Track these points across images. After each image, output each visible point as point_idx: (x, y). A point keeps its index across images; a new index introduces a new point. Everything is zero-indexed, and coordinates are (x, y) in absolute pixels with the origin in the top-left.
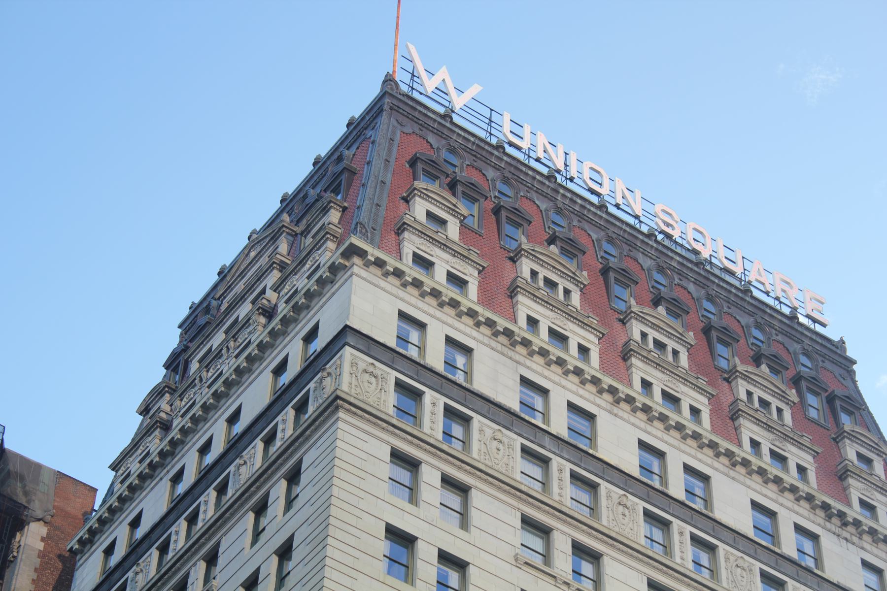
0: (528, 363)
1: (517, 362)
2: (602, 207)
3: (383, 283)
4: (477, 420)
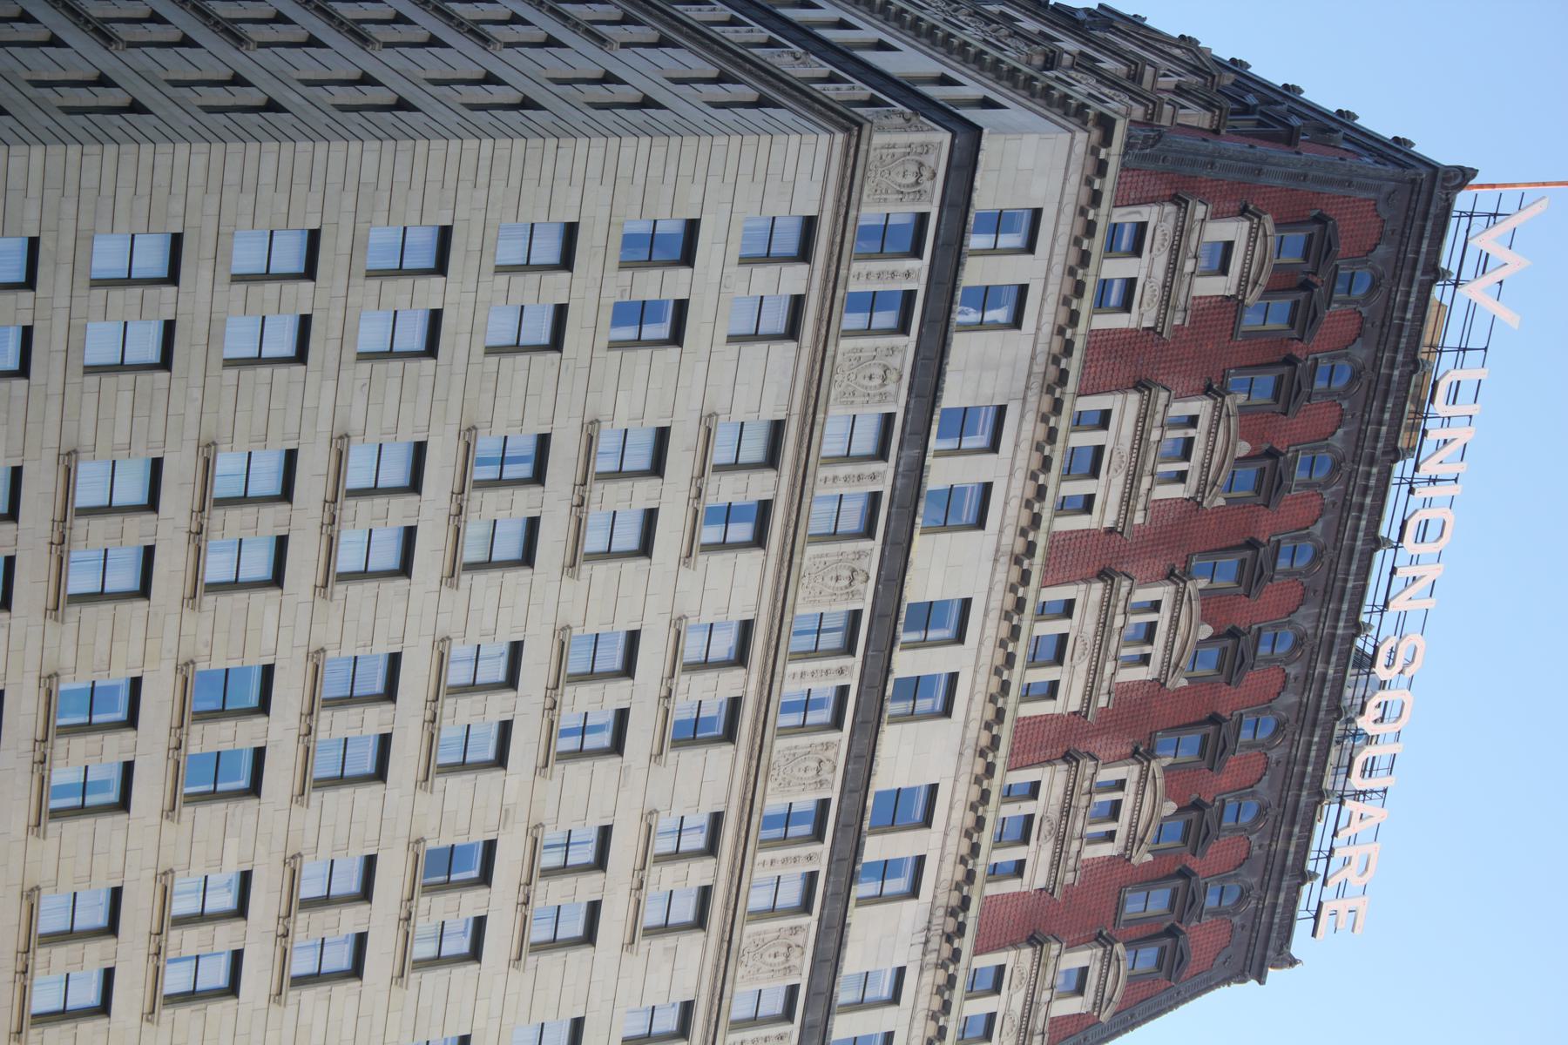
0: (1031, 417)
1: (1024, 399)
2: (1377, 543)
3: (1075, 179)
4: (909, 342)
